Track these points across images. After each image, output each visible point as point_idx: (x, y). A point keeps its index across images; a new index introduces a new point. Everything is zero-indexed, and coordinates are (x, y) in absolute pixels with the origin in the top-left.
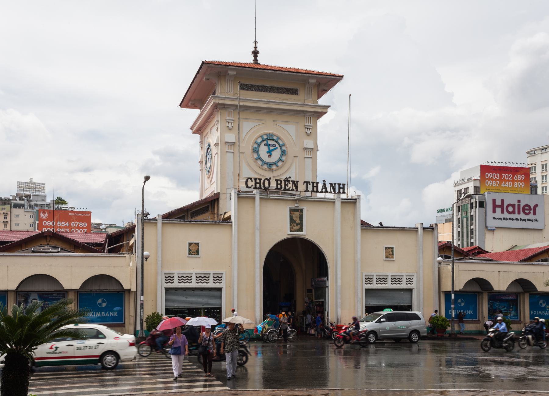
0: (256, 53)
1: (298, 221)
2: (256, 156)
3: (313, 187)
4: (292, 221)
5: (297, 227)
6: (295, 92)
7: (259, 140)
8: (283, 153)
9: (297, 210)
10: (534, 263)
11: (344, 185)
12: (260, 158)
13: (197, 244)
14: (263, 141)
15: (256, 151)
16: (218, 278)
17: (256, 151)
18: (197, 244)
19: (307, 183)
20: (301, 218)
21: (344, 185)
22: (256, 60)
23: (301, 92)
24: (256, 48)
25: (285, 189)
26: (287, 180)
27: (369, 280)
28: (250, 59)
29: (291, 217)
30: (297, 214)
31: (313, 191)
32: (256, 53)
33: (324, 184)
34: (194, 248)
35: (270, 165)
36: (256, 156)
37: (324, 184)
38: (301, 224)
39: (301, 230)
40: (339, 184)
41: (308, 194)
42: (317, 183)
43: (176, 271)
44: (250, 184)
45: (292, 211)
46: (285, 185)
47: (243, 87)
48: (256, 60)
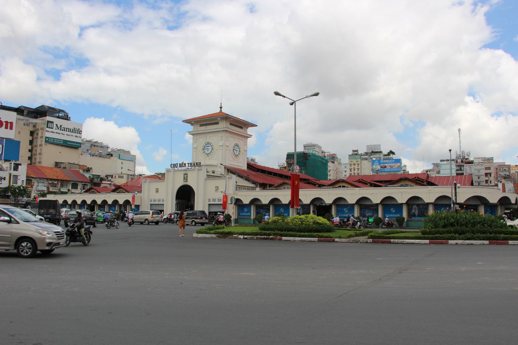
0: (221, 108)
4: (184, 178)
6: (218, 123)
8: (212, 149)
16: (163, 201)
17: (204, 149)
19: (188, 164)
22: (221, 110)
27: (209, 200)
28: (218, 110)
30: (186, 175)
32: (221, 108)
35: (208, 154)
39: (187, 181)
43: (152, 198)
45: (185, 174)
47: (201, 125)
48: (221, 110)
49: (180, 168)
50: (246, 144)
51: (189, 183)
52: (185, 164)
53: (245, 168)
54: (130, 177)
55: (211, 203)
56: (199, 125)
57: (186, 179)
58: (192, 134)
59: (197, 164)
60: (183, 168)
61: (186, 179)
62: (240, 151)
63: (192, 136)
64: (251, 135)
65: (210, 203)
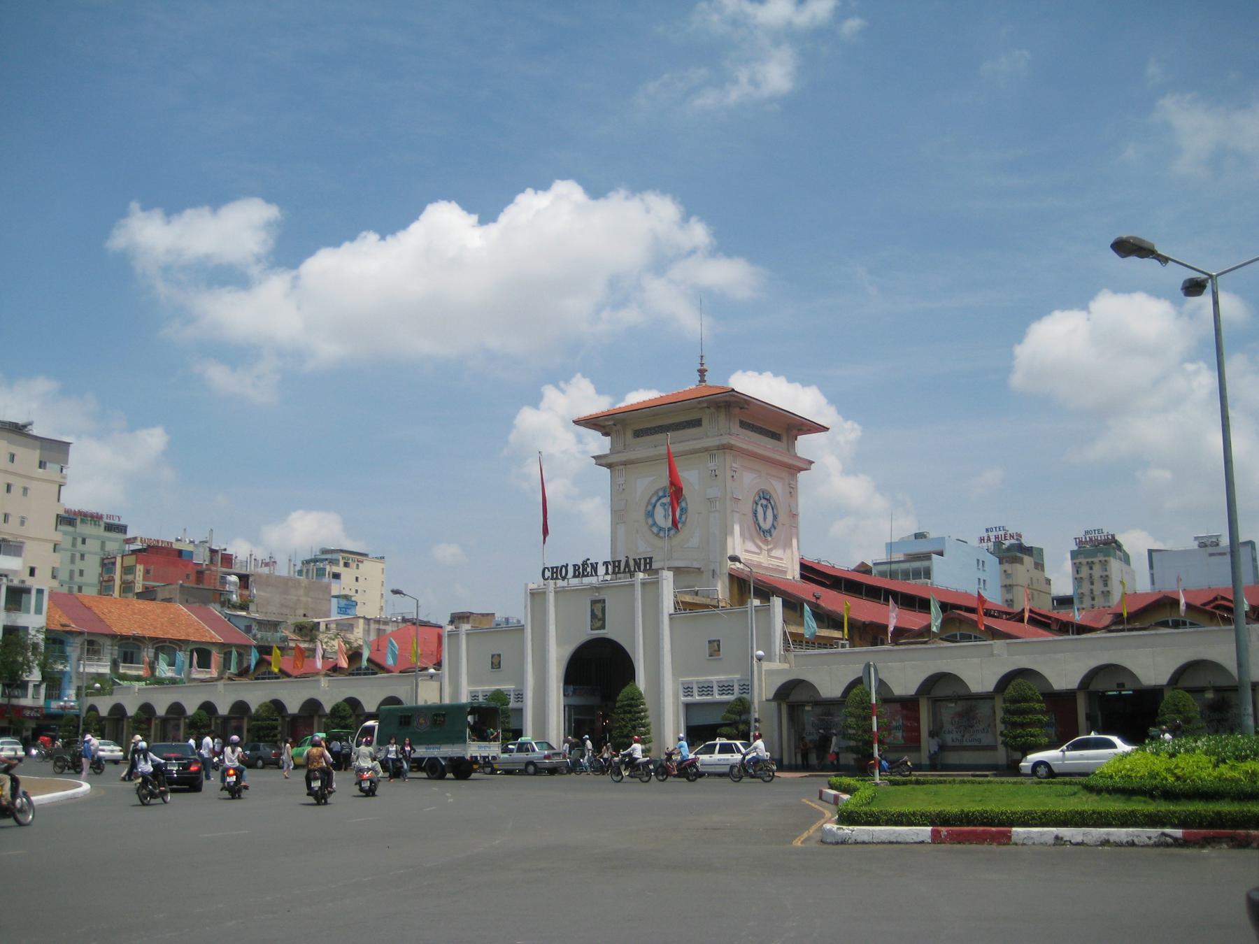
0: (702, 372)
1: (600, 615)
2: (650, 521)
3: (614, 567)
4: (593, 616)
5: (599, 624)
6: (697, 423)
7: (654, 500)
9: (599, 601)
10: (1137, 625)
11: (651, 559)
12: (655, 524)
13: (499, 655)
14: (660, 498)
15: (650, 514)
18: (499, 655)
19: (606, 563)
20: (603, 610)
21: (651, 559)
22: (702, 380)
23: (705, 422)
24: (702, 364)
25: (584, 576)
26: (585, 564)
29: (592, 611)
30: (599, 605)
31: (614, 572)
32: (702, 372)
33: (627, 562)
34: (496, 662)
36: (650, 521)
37: (627, 562)
38: (603, 619)
39: (603, 627)
40: (645, 559)
41: (608, 577)
42: (619, 562)
44: (548, 574)
45: (594, 602)
46: (584, 569)
47: (638, 434)
49: (576, 581)
50: (792, 492)
51: (610, 632)
52: (594, 567)
53: (794, 573)
54: (373, 626)
55: (697, 698)
56: (629, 434)
57: (598, 618)
58: (609, 466)
59: (637, 564)
60: (586, 580)
61: (598, 618)
62: (775, 517)
63: (606, 472)
64: (811, 462)
65: (689, 699)
